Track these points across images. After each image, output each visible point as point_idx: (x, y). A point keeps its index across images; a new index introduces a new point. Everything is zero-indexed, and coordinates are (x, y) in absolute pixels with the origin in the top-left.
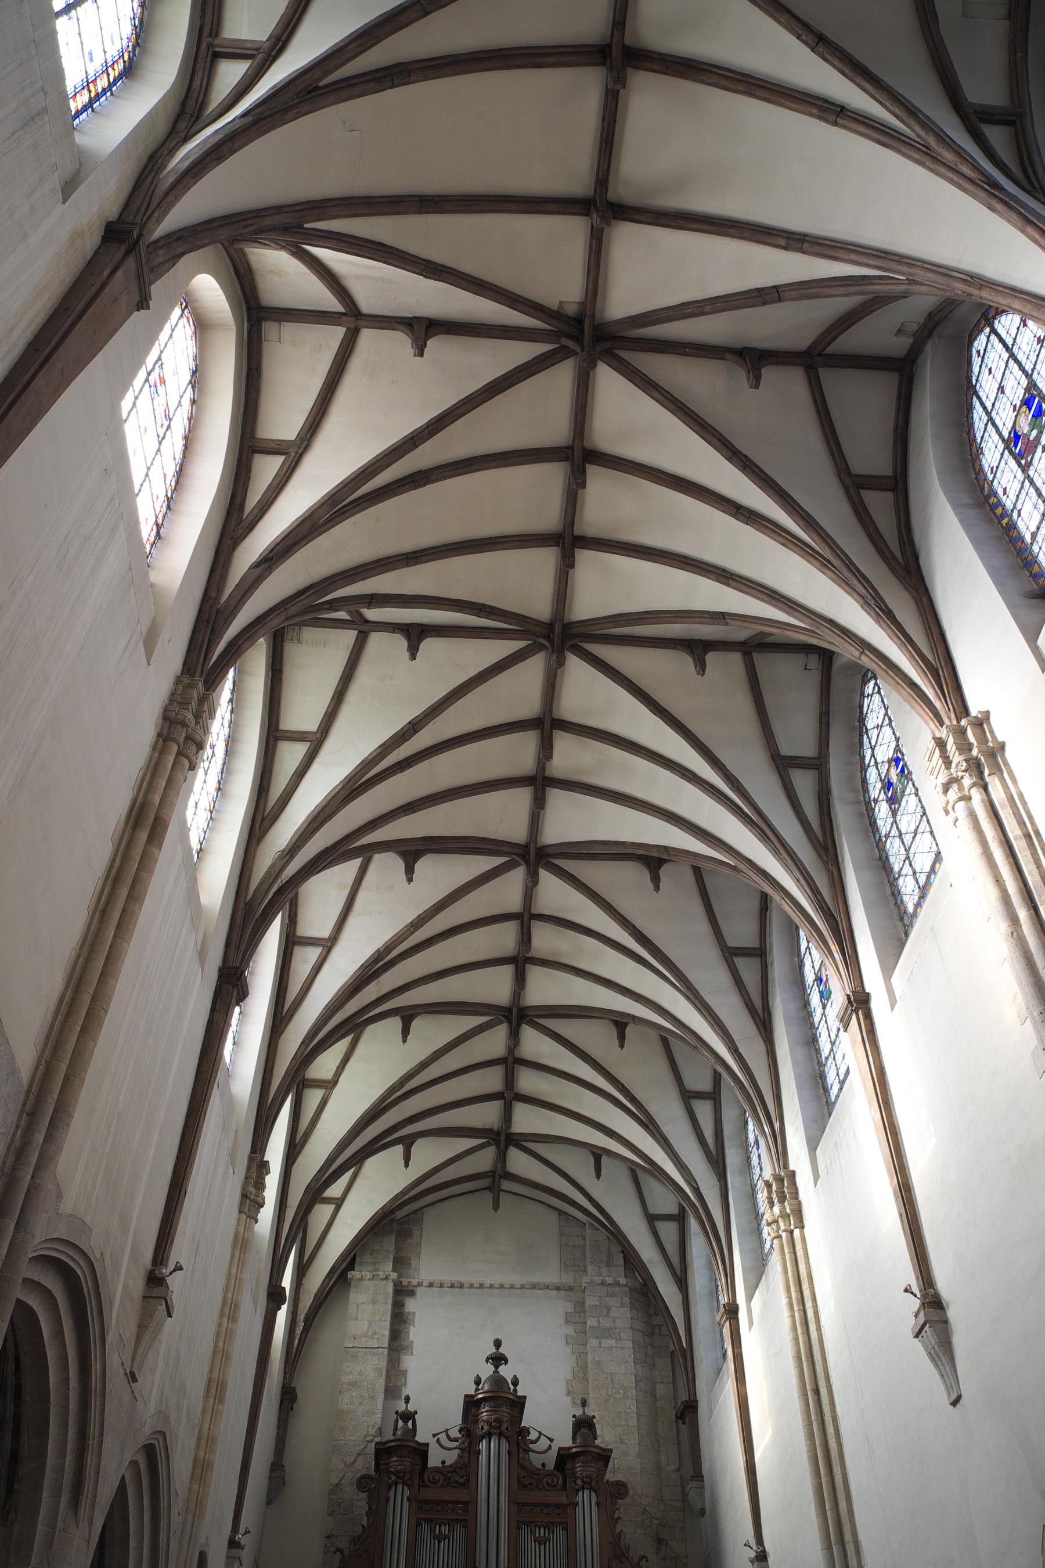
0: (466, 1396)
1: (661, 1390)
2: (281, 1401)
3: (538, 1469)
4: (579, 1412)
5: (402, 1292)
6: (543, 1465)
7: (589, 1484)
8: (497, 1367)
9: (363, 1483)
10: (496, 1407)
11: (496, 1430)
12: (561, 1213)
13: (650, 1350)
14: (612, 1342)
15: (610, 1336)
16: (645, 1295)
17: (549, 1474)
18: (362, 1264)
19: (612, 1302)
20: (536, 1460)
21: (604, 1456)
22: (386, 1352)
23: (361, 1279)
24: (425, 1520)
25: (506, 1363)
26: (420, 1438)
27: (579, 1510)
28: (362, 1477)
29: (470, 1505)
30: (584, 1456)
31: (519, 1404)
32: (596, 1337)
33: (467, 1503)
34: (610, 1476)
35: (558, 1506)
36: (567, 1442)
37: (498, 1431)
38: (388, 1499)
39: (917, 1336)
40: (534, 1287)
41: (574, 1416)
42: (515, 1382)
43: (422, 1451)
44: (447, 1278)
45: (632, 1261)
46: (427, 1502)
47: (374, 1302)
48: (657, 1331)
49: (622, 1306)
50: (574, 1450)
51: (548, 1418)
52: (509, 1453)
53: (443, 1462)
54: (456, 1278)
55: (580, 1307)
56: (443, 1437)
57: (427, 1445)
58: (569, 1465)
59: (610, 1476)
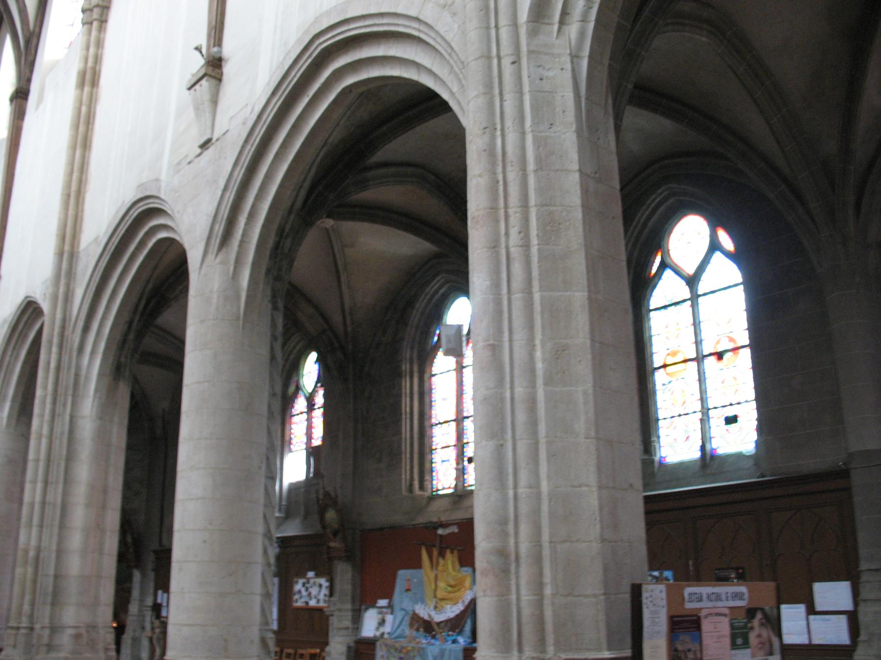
39: (189, 89)
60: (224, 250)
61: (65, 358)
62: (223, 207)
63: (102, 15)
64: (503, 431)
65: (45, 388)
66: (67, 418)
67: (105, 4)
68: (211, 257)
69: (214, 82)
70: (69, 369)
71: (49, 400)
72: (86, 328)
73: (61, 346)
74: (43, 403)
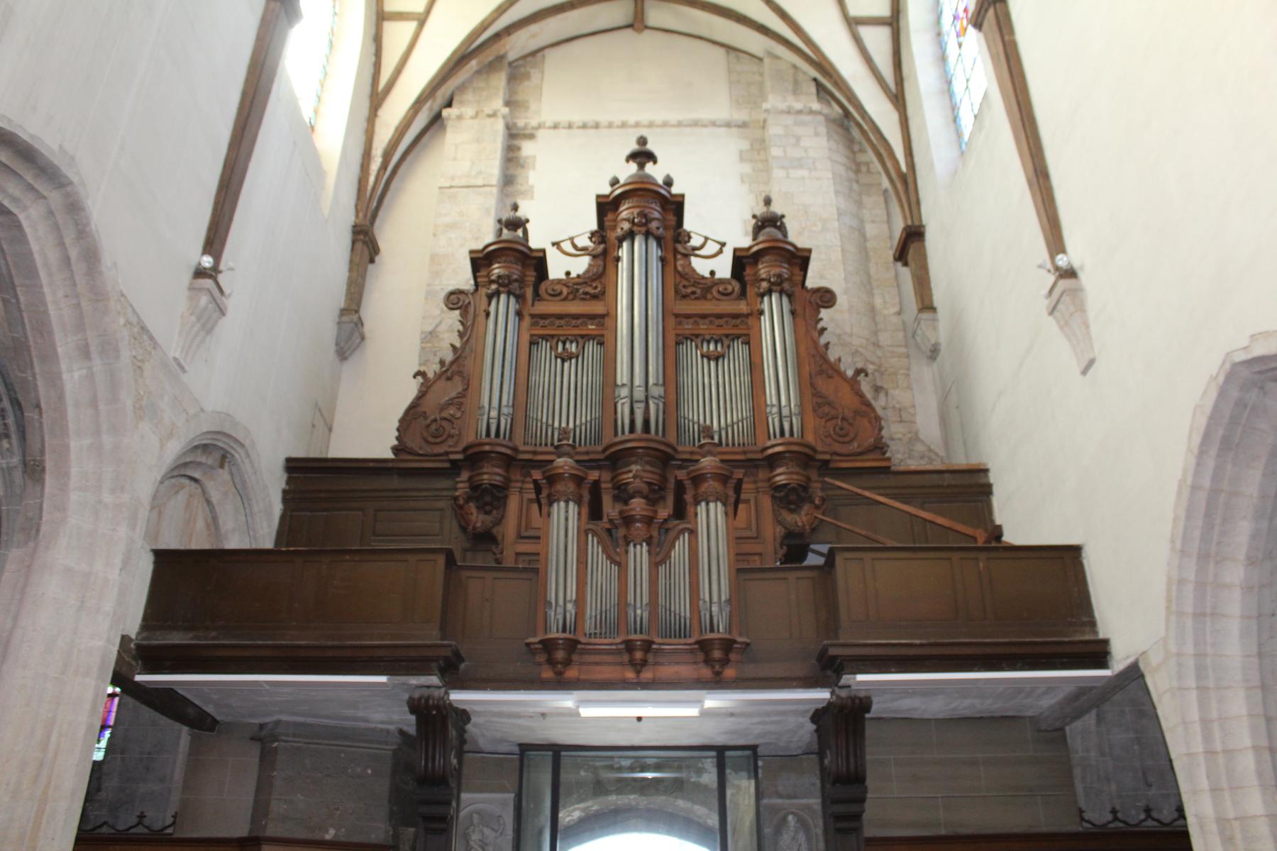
0: (598, 197)
1: (871, 230)
2: (354, 242)
3: (703, 278)
4: (760, 210)
5: (514, 136)
6: (712, 273)
7: (777, 286)
8: (641, 166)
9: (455, 300)
10: (644, 210)
11: (642, 228)
12: (729, 48)
13: (855, 186)
14: (804, 173)
15: (801, 167)
16: (849, 122)
17: (722, 281)
18: (462, 103)
19: (800, 131)
20: (701, 266)
21: (801, 259)
22: (495, 190)
23: (460, 117)
24: (544, 337)
25: (655, 162)
26: (534, 243)
27: (765, 320)
28: (452, 293)
29: (605, 319)
30: (774, 258)
31: (675, 206)
32: (783, 168)
33: (603, 316)
34: (811, 282)
35: (735, 316)
36: (745, 241)
37: (643, 229)
38: (488, 314)
40: (695, 124)
41: (754, 216)
42: (669, 182)
43: (538, 262)
44: (577, 118)
45: (827, 82)
46: (544, 317)
47: (478, 141)
48: (864, 169)
49: (816, 134)
50: (755, 249)
51: (718, 225)
52: (663, 260)
53: (568, 274)
54: (589, 118)
55: (760, 145)
56: (567, 246)
57: (544, 251)
58: (748, 271)
59: (811, 282)
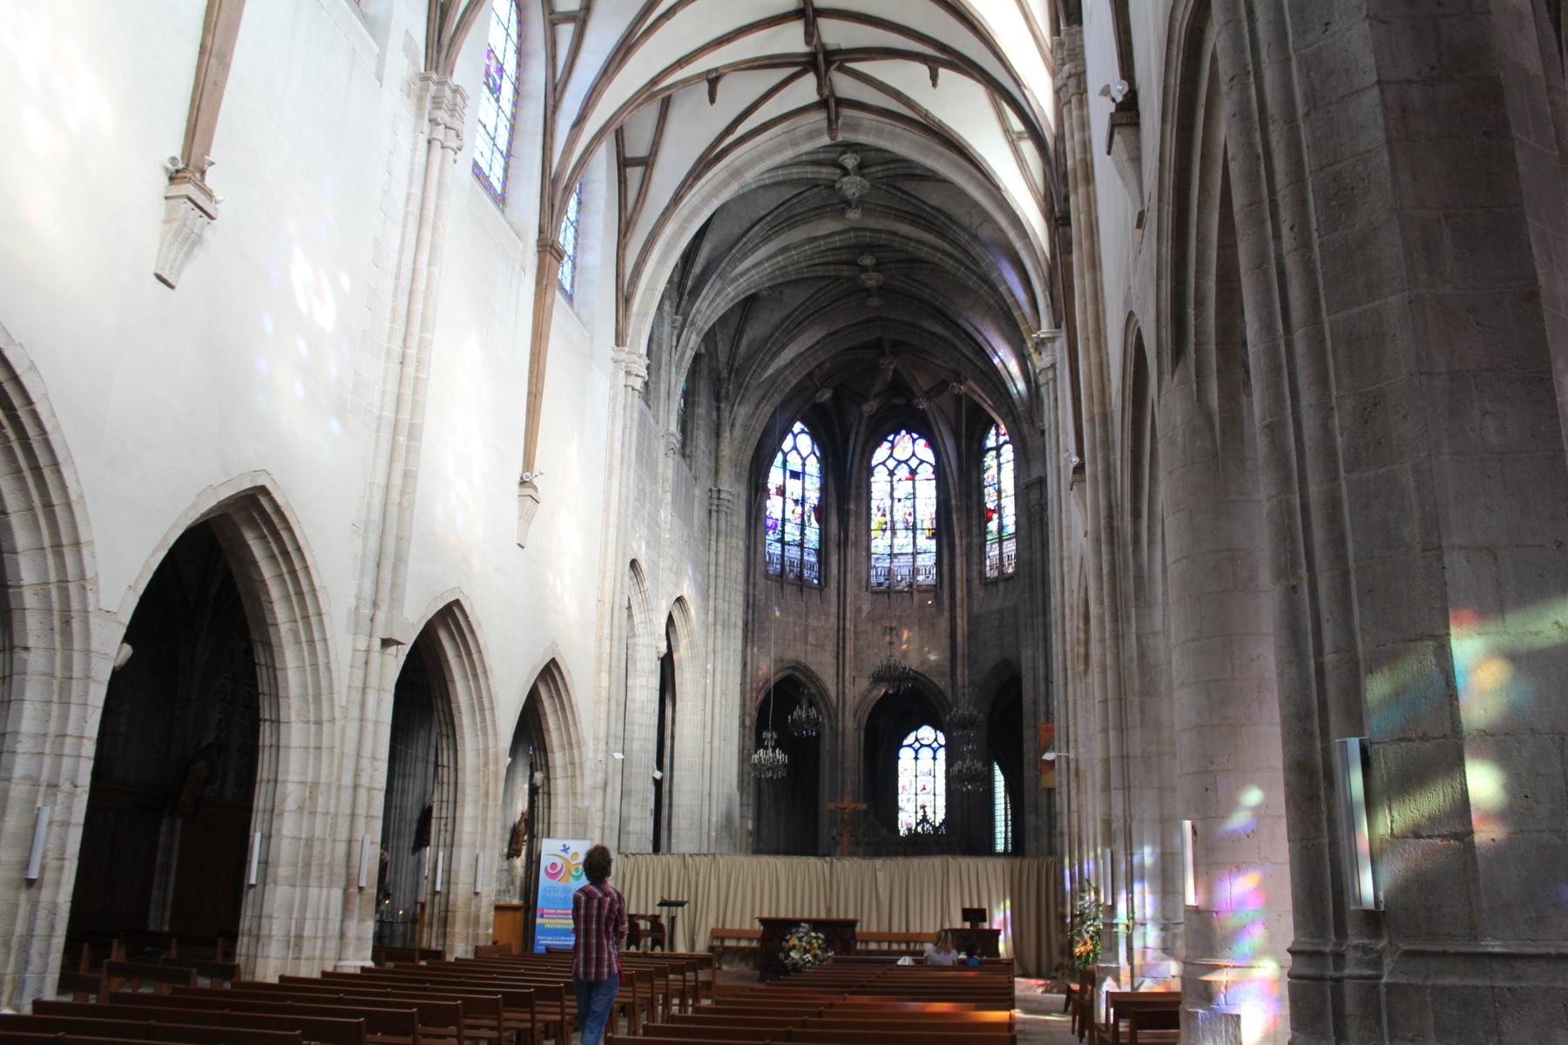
60: (1181, 364)
61: (1119, 557)
62: (1163, 303)
63: (1078, 86)
64: (1294, 563)
65: (1101, 603)
66: (1134, 637)
67: (1080, 69)
68: (1167, 377)
69: (1128, 131)
70: (1126, 570)
71: (1107, 619)
72: (1136, 514)
73: (1111, 543)
74: (1102, 622)
